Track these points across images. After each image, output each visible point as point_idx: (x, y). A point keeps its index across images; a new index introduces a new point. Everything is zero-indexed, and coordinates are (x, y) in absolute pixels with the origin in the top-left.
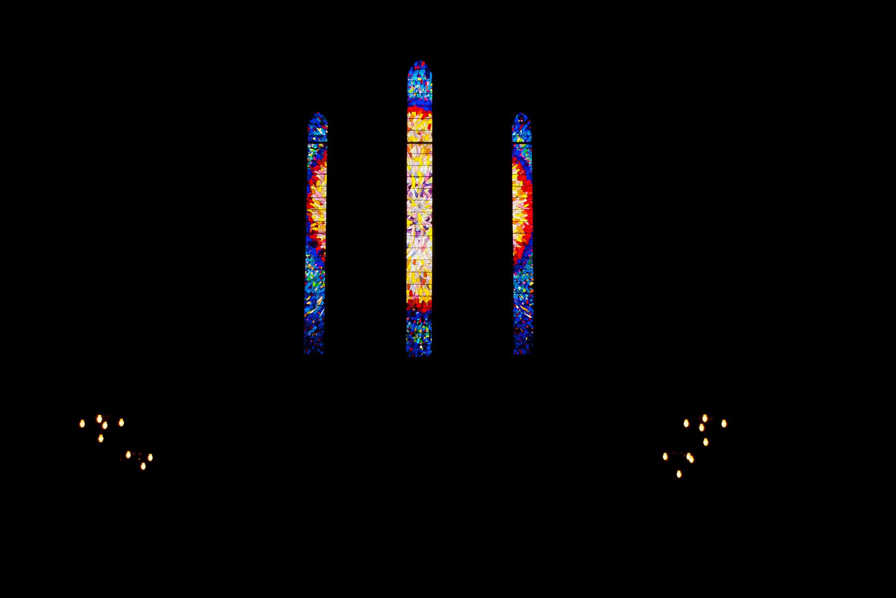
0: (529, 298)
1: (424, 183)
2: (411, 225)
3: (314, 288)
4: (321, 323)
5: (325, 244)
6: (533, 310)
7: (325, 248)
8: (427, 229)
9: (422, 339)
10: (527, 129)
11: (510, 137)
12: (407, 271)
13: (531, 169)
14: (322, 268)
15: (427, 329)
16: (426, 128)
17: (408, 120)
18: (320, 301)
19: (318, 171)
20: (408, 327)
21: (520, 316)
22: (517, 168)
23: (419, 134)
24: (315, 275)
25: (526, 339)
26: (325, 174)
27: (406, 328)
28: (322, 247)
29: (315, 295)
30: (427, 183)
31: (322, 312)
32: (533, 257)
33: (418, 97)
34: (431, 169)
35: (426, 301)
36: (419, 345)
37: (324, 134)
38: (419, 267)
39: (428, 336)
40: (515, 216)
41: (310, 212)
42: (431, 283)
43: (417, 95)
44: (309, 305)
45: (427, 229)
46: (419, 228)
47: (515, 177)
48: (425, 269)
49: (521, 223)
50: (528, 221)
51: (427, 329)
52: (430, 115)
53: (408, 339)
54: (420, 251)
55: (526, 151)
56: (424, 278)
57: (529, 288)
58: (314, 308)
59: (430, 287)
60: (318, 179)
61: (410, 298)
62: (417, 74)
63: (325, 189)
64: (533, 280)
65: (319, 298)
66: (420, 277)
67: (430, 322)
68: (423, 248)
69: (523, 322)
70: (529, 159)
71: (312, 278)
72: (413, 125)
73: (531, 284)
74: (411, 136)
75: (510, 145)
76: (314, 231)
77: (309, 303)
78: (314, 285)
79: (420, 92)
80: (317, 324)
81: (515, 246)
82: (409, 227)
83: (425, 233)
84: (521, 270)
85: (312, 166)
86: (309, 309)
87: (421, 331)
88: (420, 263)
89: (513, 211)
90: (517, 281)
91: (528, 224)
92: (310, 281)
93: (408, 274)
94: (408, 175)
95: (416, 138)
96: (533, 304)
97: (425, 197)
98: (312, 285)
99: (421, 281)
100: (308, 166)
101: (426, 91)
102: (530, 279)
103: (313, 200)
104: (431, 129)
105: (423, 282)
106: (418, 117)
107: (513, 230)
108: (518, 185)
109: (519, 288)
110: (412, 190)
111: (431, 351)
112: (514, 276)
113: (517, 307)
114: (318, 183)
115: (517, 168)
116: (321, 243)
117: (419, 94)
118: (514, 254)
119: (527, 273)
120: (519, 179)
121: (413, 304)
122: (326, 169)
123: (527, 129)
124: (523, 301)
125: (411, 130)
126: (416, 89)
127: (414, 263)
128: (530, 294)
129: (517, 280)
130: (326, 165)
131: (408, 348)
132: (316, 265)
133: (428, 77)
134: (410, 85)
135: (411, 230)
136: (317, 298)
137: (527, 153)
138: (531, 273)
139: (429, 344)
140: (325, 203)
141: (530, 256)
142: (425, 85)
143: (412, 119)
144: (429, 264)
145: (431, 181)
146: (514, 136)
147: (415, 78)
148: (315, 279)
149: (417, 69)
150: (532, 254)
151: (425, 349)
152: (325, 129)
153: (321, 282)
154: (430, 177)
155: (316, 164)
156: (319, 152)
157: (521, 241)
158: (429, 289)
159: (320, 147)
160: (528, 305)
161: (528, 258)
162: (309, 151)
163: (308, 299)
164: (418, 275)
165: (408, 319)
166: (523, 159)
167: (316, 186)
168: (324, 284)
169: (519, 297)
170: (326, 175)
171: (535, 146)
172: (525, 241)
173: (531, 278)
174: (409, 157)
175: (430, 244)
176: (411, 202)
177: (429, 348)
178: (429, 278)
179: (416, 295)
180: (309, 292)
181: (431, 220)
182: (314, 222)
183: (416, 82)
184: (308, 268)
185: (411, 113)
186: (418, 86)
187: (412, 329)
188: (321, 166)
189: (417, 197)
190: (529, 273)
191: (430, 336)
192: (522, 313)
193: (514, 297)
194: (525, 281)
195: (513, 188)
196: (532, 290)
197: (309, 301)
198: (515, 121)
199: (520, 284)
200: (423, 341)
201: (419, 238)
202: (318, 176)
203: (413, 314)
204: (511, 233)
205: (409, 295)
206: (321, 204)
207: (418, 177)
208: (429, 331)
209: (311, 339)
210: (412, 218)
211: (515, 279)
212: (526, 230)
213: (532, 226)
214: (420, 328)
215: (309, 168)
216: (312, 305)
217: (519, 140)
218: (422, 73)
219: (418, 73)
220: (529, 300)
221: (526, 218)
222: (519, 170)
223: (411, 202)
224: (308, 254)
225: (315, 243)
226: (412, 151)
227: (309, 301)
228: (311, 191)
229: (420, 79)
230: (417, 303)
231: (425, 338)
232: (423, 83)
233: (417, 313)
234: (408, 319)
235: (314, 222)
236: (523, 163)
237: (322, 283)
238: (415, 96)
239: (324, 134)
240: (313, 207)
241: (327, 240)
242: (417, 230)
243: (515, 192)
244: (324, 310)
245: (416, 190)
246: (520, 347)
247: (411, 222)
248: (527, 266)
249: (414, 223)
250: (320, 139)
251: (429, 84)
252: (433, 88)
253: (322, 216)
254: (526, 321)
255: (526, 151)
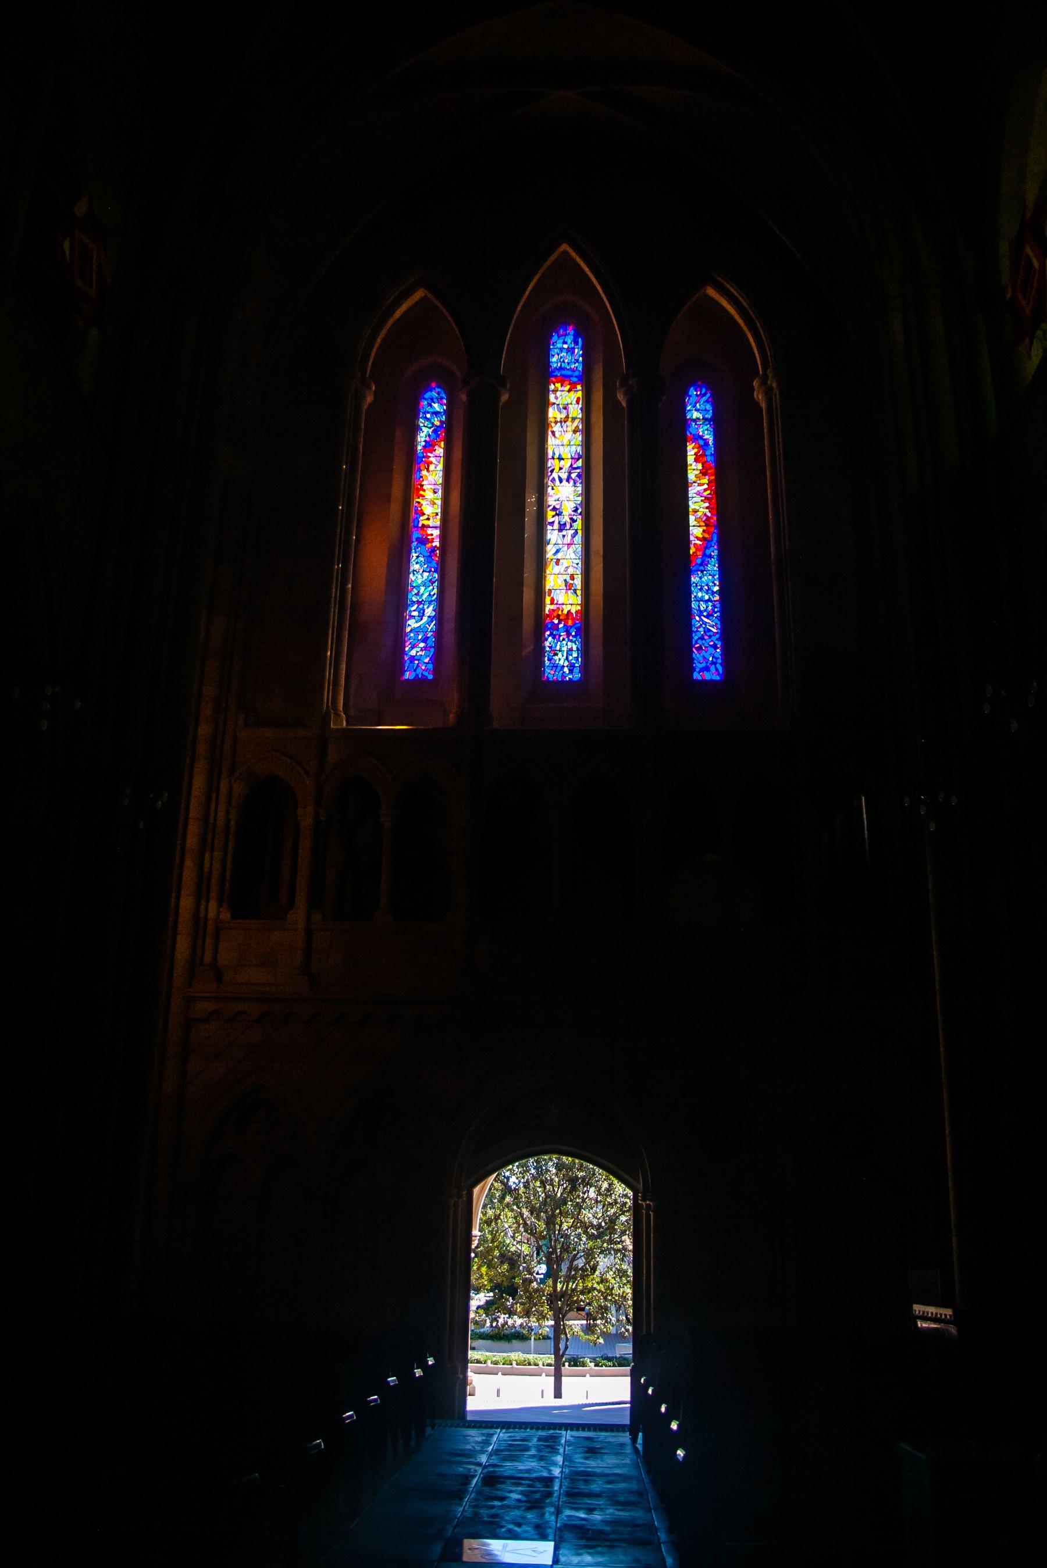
0: (714, 606)
1: (571, 465)
2: (553, 516)
3: (423, 594)
4: (430, 639)
5: (438, 540)
6: (719, 623)
7: (438, 546)
8: (576, 521)
9: (567, 658)
10: (707, 401)
11: (684, 412)
12: (548, 572)
13: (713, 449)
14: (433, 570)
15: (575, 648)
16: (574, 402)
17: (551, 392)
18: (429, 611)
19: (432, 453)
20: (547, 644)
21: (701, 629)
22: (693, 448)
23: (565, 408)
24: (424, 579)
25: (711, 659)
26: (441, 457)
27: (545, 647)
28: (434, 544)
29: (424, 605)
30: (575, 466)
31: (432, 624)
32: (718, 556)
33: (563, 366)
34: (579, 449)
35: (573, 611)
36: (563, 666)
37: (442, 410)
38: (563, 568)
39: (575, 655)
40: (692, 506)
41: (419, 503)
42: (579, 587)
43: (563, 364)
44: (414, 616)
45: (573, 521)
46: (564, 520)
47: (691, 459)
48: (571, 571)
49: (700, 514)
50: (709, 511)
51: (575, 648)
52: (579, 387)
53: (548, 660)
54: (566, 548)
55: (705, 427)
56: (571, 582)
57: (712, 595)
58: (422, 619)
59: (579, 592)
60: (431, 463)
61: (552, 607)
62: (562, 341)
63: (441, 474)
64: (718, 584)
65: (428, 607)
66: (565, 580)
67: (578, 637)
68: (569, 545)
69: (706, 637)
70: (709, 437)
71: (419, 582)
72: (556, 398)
73: (716, 589)
74: (552, 413)
75: (685, 423)
76: (423, 525)
77: (414, 614)
78: (421, 592)
79: (566, 361)
80: (425, 640)
81: (693, 542)
82: (550, 520)
83: (571, 526)
84: (702, 571)
85: (424, 447)
86: (414, 621)
87: (565, 649)
88: (564, 563)
89: (690, 499)
90: (696, 586)
91: (709, 515)
92: (417, 586)
93: (548, 577)
94: (550, 457)
95: (561, 413)
96: (718, 614)
97: (572, 482)
98: (419, 592)
99: (566, 586)
100: (419, 448)
101: (573, 360)
102: (713, 582)
103: (424, 487)
104: (581, 403)
105: (568, 586)
106: (563, 388)
107: (690, 522)
108: (695, 468)
109: (700, 594)
110: (555, 475)
111: (580, 674)
112: (692, 579)
113: (697, 618)
114: (432, 467)
115: (693, 448)
116: (433, 539)
117: (564, 361)
118: (691, 553)
119: (710, 575)
120: (696, 460)
121: (555, 614)
122: (442, 450)
123: (707, 401)
124: (705, 610)
125: (554, 404)
126: (561, 357)
127: (558, 562)
128: (714, 601)
129: (696, 584)
130: (442, 446)
131: (548, 670)
132: (426, 566)
133: (576, 343)
134: (553, 354)
135: (553, 522)
136: (425, 607)
137: (707, 430)
138: (715, 575)
139: (576, 665)
140: (440, 491)
141: (713, 554)
142: (574, 352)
143: (555, 391)
144: (577, 564)
145: (579, 463)
146: (689, 410)
147: (559, 345)
148: (424, 584)
149: (562, 335)
150: (716, 552)
151: (571, 671)
152: (442, 404)
153: (431, 588)
154: (578, 459)
155: (430, 446)
156: (433, 432)
157: (701, 536)
158: (577, 596)
159: (436, 426)
160: (713, 616)
161: (710, 556)
162: (421, 430)
163: (413, 609)
164: (562, 578)
165: (548, 633)
166: (701, 437)
167: (428, 470)
168: (435, 591)
169: (699, 606)
170: (442, 458)
171: (716, 422)
172: (706, 536)
173: (715, 582)
174: (551, 435)
175: (578, 539)
176: (553, 489)
177: (576, 670)
178: (578, 582)
179: (559, 603)
180: (414, 599)
181: (579, 511)
182: (424, 514)
183: (561, 349)
184: (414, 571)
185: (554, 385)
186: (564, 354)
187: (554, 646)
188: (436, 447)
189: (561, 481)
190: (713, 576)
191: (578, 654)
192: (704, 626)
193: (693, 606)
194: (707, 585)
195: (689, 472)
196: (717, 598)
197: (414, 611)
198: (690, 393)
199: (701, 590)
200: (568, 661)
201: (564, 533)
202: (431, 459)
203: (556, 627)
204: (688, 526)
205: (549, 603)
206: (435, 492)
207: (563, 459)
208: (578, 649)
209: (416, 660)
210: (554, 509)
211: (694, 583)
212: (707, 522)
213: (715, 518)
214: (565, 645)
215: (421, 450)
216: (419, 616)
217: (696, 415)
218: (569, 339)
219: (564, 340)
220: (713, 610)
221: (707, 508)
222: (696, 450)
223: (553, 489)
224: (416, 552)
225: (424, 541)
226: (554, 429)
227: (414, 611)
228: (422, 477)
229: (565, 346)
230: (560, 613)
231: (570, 658)
232: (571, 351)
233: (561, 626)
234: (548, 633)
235: (424, 514)
236: (701, 442)
237: (433, 588)
238: (559, 365)
239: (442, 410)
240: (424, 496)
241: (443, 537)
242: (562, 523)
243: (691, 476)
244: (434, 622)
245: (560, 474)
246: (702, 670)
247: (554, 513)
248: (709, 567)
249: (556, 514)
250: (436, 416)
251: (578, 351)
252: (582, 356)
253: (435, 506)
254: (710, 637)
255: (705, 427)
